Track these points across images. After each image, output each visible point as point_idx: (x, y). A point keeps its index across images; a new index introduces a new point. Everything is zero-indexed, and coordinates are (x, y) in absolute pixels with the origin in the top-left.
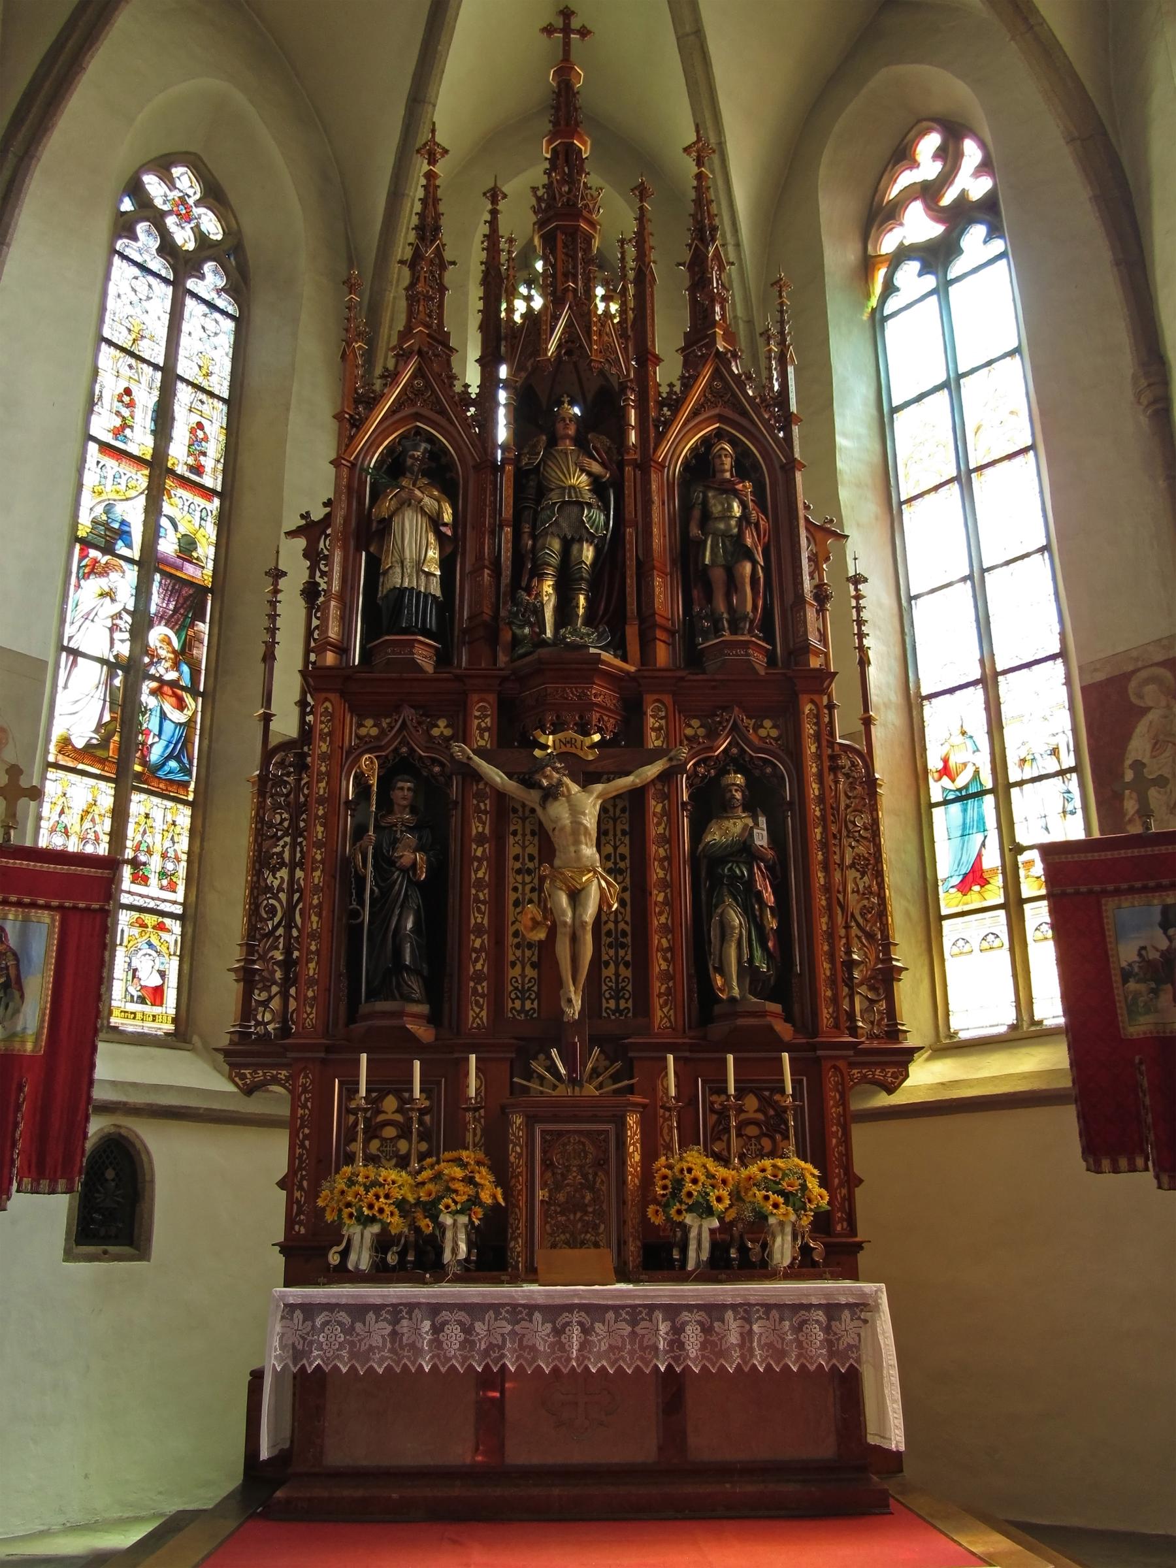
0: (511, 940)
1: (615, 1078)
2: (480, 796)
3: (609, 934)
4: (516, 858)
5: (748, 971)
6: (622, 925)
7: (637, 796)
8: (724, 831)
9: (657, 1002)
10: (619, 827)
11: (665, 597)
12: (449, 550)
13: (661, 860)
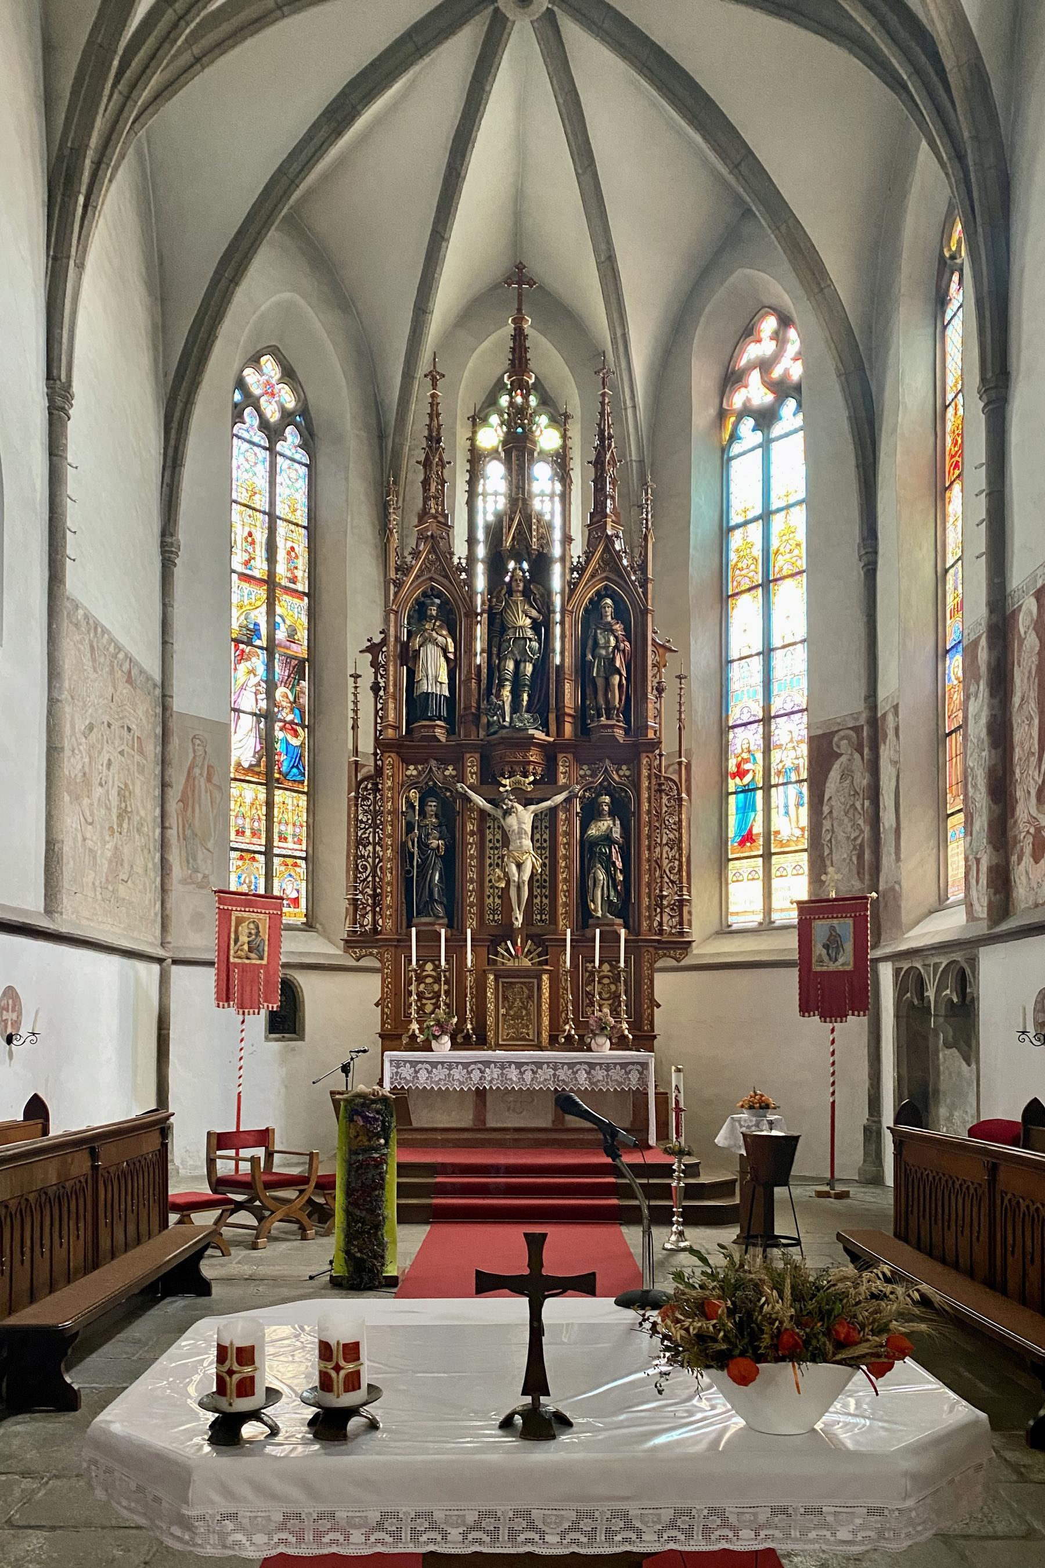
0: (487, 884)
1: (539, 955)
2: (472, 810)
3: (537, 881)
4: (490, 841)
5: (607, 903)
6: (544, 877)
7: (553, 811)
8: (599, 828)
9: (561, 918)
10: (544, 824)
12: (452, 665)
13: (565, 844)
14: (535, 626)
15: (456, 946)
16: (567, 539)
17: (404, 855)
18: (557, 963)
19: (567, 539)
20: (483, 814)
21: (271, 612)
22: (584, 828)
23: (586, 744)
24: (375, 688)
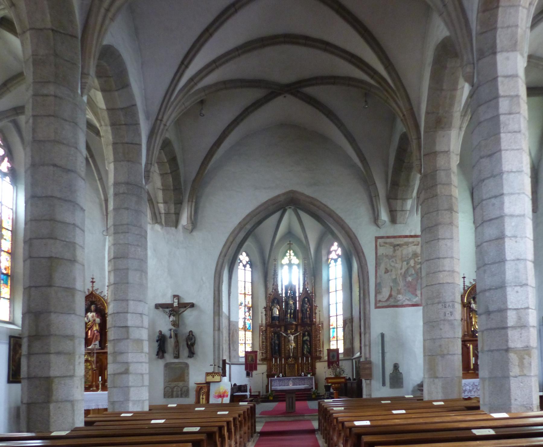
7: (297, 336)
11: (300, 315)
15: (281, 360)
17: (271, 344)
18: (298, 362)
20: (285, 337)
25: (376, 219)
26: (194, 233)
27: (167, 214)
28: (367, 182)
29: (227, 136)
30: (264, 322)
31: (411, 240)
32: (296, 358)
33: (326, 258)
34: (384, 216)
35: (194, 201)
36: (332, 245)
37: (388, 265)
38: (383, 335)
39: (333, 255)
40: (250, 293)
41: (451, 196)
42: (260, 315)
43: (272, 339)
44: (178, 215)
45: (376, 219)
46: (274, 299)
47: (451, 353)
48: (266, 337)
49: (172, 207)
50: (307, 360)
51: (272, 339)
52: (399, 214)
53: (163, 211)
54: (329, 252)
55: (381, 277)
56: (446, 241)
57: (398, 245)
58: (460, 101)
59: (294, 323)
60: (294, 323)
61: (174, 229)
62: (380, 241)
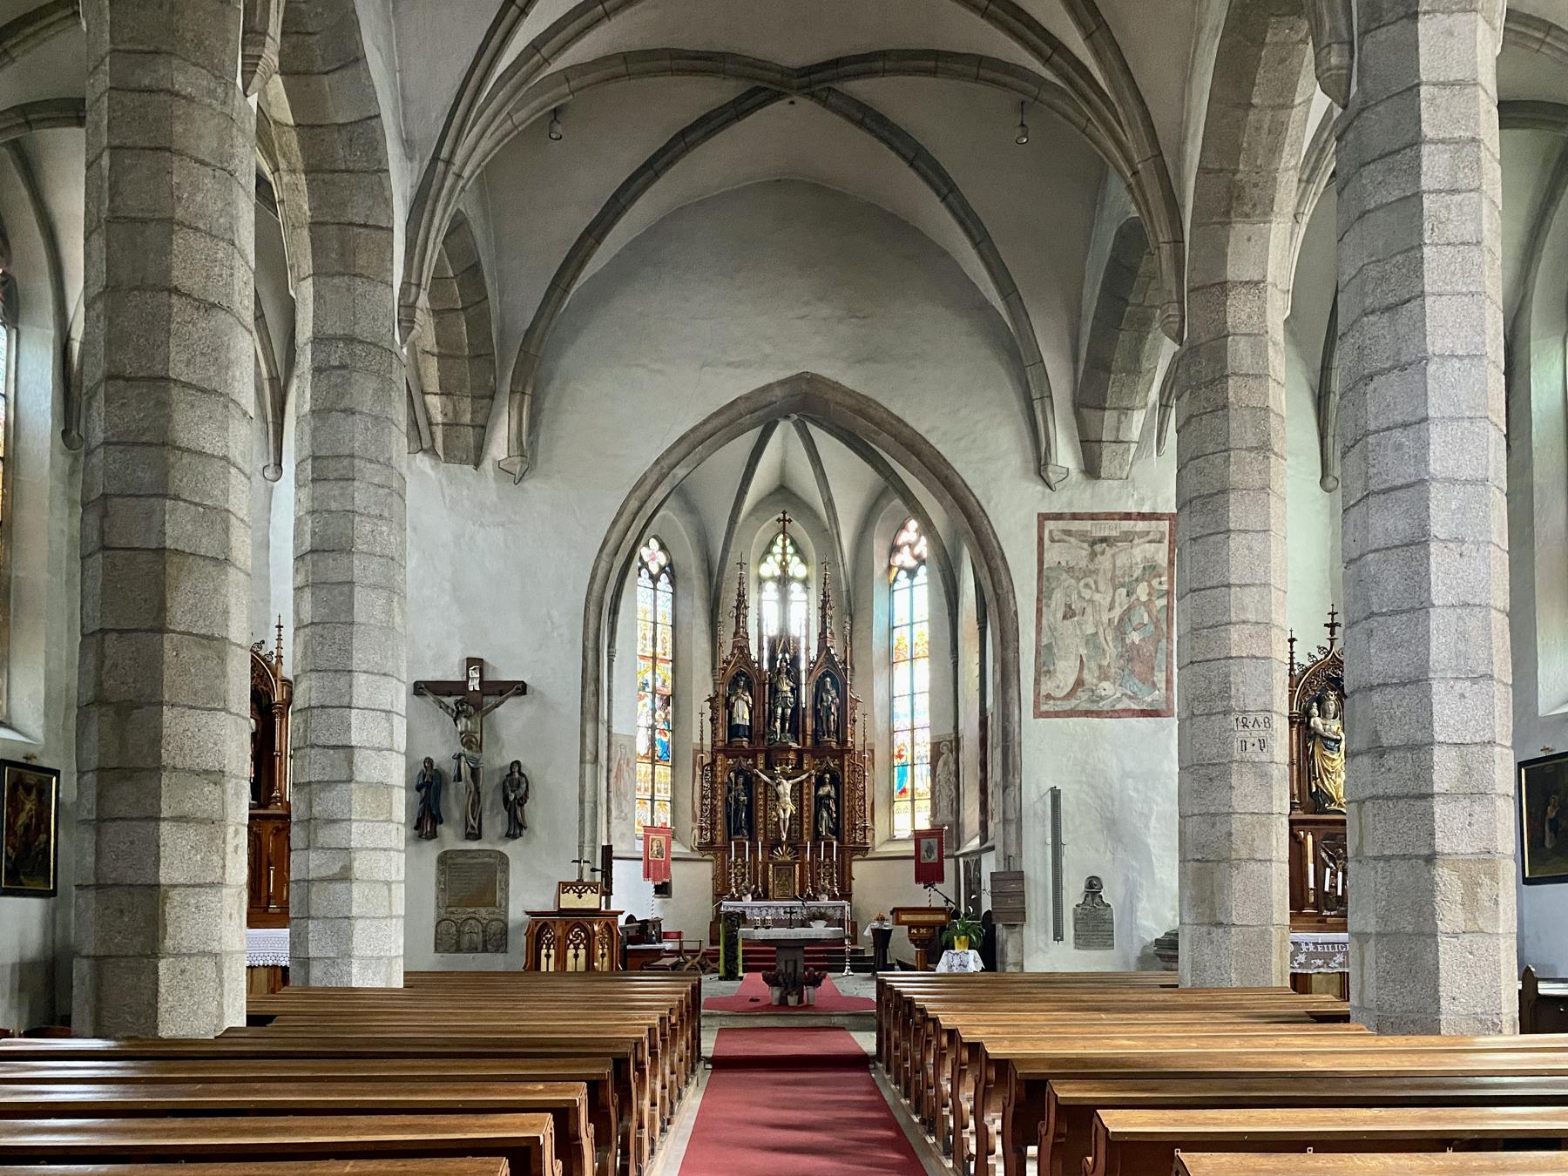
7: (801, 783)
14: (792, 690)
15: (754, 850)
16: (808, 649)
17: (727, 804)
18: (803, 857)
19: (808, 649)
20: (766, 784)
21: (654, 673)
22: (817, 790)
23: (819, 750)
24: (712, 720)
25: (1041, 465)
26: (528, 484)
27: (451, 426)
28: (1019, 359)
29: (625, 209)
30: (708, 741)
31: (1141, 526)
32: (796, 846)
33: (885, 565)
34: (1065, 455)
35: (529, 391)
36: (903, 527)
37: (1075, 597)
38: (1056, 795)
39: (904, 558)
40: (669, 657)
41: (1267, 409)
42: (696, 718)
43: (730, 791)
44: (482, 430)
45: (1041, 465)
46: (738, 675)
47: (1258, 856)
48: (712, 783)
49: (466, 405)
50: (829, 855)
51: (730, 791)
52: (1107, 451)
53: (439, 418)
54: (894, 549)
55: (1052, 629)
56: (1249, 536)
57: (1104, 540)
58: (1299, 141)
59: (794, 745)
60: (794, 745)
61: (470, 468)
62: (1050, 525)
